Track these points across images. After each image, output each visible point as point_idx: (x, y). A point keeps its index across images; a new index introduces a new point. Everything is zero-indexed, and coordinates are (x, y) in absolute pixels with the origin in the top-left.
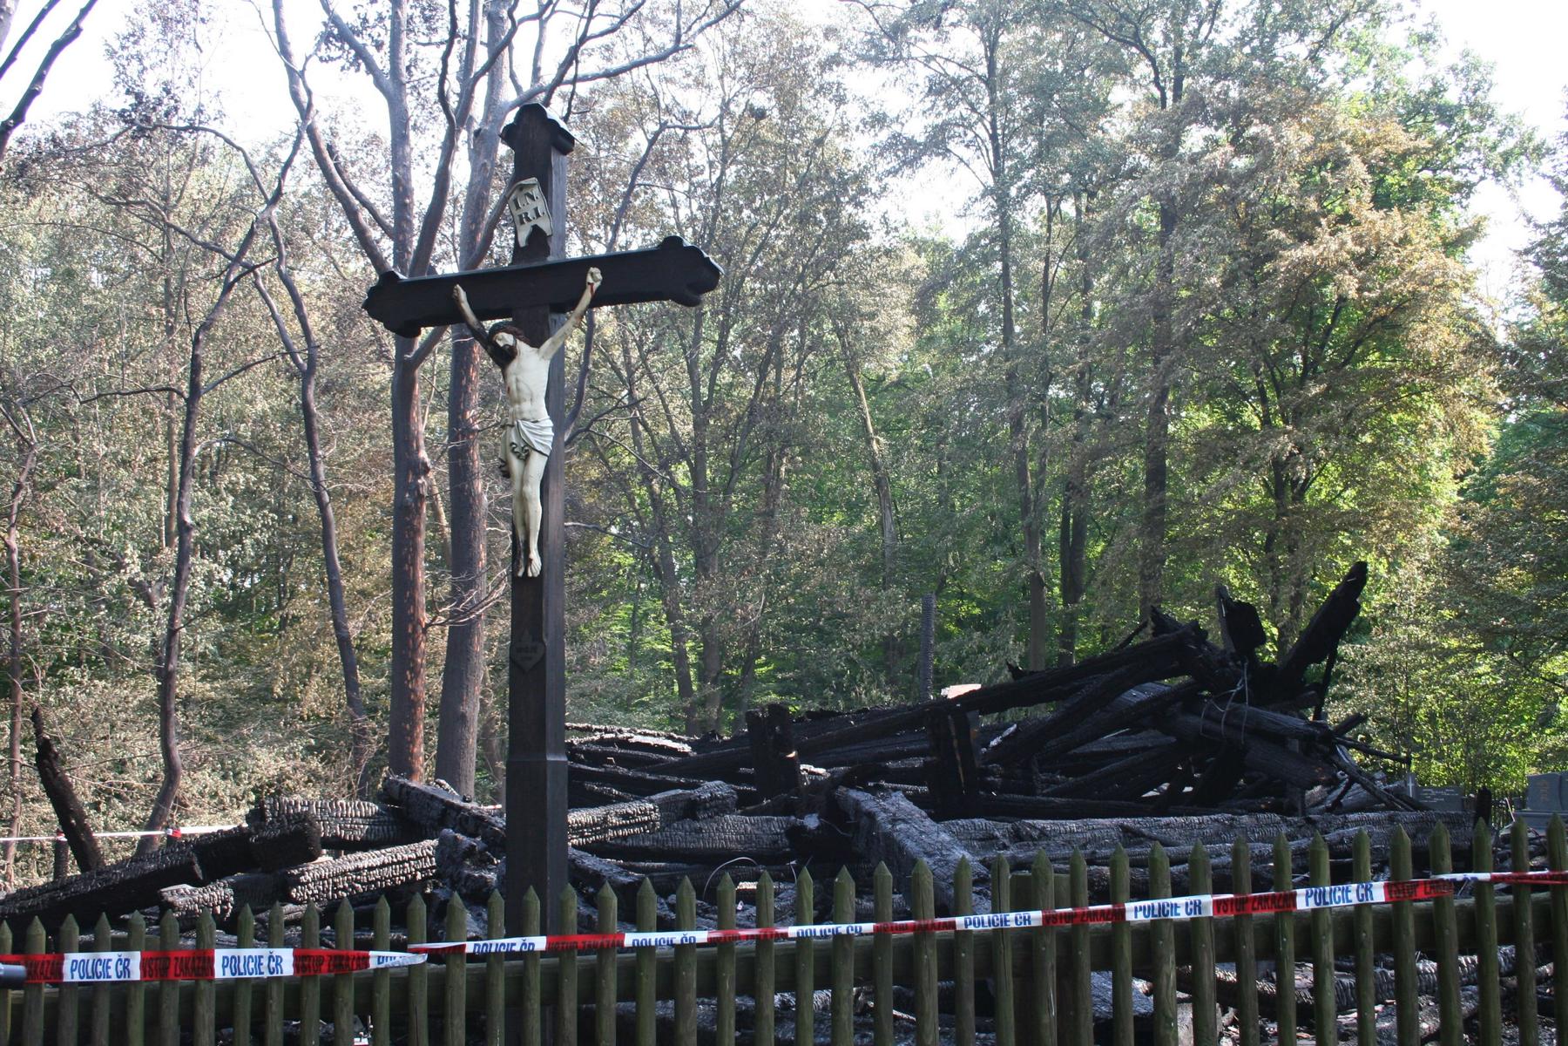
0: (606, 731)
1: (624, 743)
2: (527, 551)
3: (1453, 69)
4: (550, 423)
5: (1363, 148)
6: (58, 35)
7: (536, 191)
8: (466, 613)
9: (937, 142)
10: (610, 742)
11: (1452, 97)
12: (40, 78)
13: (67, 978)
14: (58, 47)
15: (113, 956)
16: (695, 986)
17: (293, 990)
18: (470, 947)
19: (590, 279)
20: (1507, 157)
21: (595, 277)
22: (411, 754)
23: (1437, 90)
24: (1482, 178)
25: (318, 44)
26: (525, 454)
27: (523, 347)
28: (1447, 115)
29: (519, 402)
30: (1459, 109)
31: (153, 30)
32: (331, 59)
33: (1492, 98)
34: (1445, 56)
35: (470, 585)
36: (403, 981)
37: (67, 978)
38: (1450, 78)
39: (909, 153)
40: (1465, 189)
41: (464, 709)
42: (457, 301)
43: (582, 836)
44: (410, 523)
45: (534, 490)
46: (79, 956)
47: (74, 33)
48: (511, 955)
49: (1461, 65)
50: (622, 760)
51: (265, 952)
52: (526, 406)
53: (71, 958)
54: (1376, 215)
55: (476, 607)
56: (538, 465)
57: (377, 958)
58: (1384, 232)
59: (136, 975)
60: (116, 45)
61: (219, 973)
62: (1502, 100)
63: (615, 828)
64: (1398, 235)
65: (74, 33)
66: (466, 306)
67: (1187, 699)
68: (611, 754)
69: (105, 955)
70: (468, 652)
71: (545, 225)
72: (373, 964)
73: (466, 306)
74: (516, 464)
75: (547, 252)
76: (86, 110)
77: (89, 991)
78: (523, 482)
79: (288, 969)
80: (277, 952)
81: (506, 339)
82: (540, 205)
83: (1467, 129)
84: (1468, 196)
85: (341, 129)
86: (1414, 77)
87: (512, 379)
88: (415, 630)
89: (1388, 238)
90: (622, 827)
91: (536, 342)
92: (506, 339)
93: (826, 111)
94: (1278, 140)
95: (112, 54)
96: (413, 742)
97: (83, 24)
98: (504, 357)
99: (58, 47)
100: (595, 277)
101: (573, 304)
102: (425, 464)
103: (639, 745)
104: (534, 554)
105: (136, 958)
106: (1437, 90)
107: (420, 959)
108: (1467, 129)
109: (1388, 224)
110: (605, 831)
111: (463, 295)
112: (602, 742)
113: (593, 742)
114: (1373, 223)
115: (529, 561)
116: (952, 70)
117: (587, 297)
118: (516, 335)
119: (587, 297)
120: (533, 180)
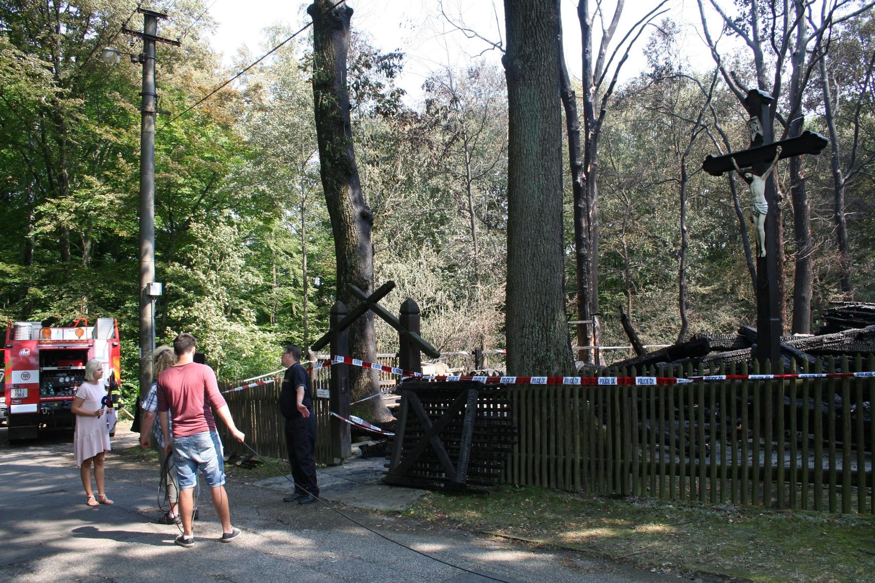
0: (851, 304)
1: (859, 309)
2: (761, 248)
4: (766, 203)
6: (620, 60)
7: (757, 121)
8: (802, 255)
10: (852, 308)
12: (616, 76)
14: (621, 64)
16: (771, 391)
17: (657, 389)
18: (704, 378)
19: (777, 150)
21: (779, 149)
22: (781, 314)
26: (758, 214)
27: (755, 177)
29: (754, 196)
31: (660, 40)
32: (731, 34)
35: (804, 244)
36: (686, 387)
41: (805, 295)
42: (732, 163)
43: (812, 346)
45: (761, 227)
46: (602, 378)
47: (626, 57)
48: (716, 380)
50: (856, 316)
51: (649, 378)
52: (757, 198)
53: (600, 378)
55: (808, 251)
56: (762, 218)
57: (679, 380)
59: (616, 383)
60: (647, 49)
61: (637, 384)
63: (826, 343)
65: (626, 57)
66: (735, 164)
68: (851, 313)
69: (608, 378)
70: (804, 271)
71: (761, 132)
72: (678, 382)
73: (735, 164)
74: (755, 218)
75: (762, 141)
76: (638, 75)
77: (605, 387)
78: (758, 224)
79: (655, 383)
80: (652, 378)
81: (749, 175)
82: (759, 126)
85: (741, 60)
88: (780, 264)
90: (829, 343)
91: (760, 174)
92: (749, 175)
95: (645, 53)
96: (781, 309)
97: (628, 54)
98: (750, 181)
99: (621, 64)
100: (779, 149)
102: (780, 196)
103: (866, 309)
104: (764, 249)
105: (616, 379)
107: (691, 381)
110: (822, 344)
111: (734, 161)
112: (849, 308)
113: (844, 309)
115: (761, 252)
117: (777, 157)
118: (753, 173)
119: (777, 157)
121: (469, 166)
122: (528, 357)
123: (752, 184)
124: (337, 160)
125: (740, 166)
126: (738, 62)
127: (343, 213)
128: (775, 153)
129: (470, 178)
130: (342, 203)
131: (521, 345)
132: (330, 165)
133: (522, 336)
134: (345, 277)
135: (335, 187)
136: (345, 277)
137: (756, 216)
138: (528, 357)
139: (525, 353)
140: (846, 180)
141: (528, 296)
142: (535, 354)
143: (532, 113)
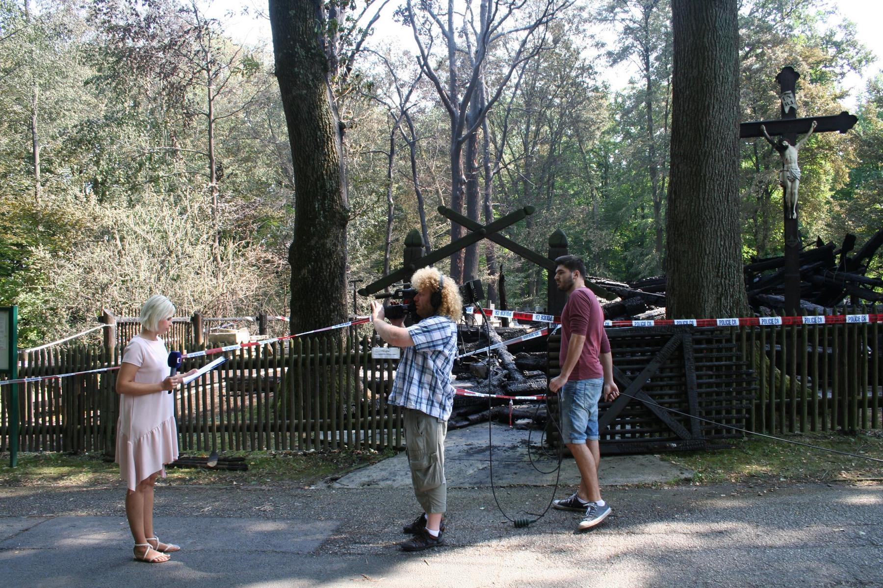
1: (603, 283)
3: (840, 26)
5: (806, 59)
6: (371, 19)
7: (791, 95)
9: (624, 53)
11: (837, 38)
13: (847, 322)
15: (860, 316)
20: (860, 62)
21: (814, 124)
23: (832, 34)
24: (849, 71)
25: (394, 16)
26: (793, 181)
28: (837, 45)
30: (842, 43)
33: (857, 37)
34: (833, 22)
37: (847, 322)
38: (838, 29)
39: (616, 58)
40: (843, 75)
42: (763, 130)
44: (459, 203)
46: (850, 316)
47: (377, 17)
49: (844, 24)
52: (793, 165)
54: (811, 86)
58: (815, 93)
59: (867, 321)
62: (860, 38)
64: (820, 94)
67: (817, 271)
69: (858, 316)
74: (789, 184)
77: (853, 325)
81: (786, 143)
83: (844, 50)
84: (842, 78)
85: (392, 48)
86: (821, 30)
87: (788, 157)
89: (816, 95)
91: (794, 144)
93: (576, 41)
94: (774, 55)
97: (380, 13)
100: (814, 124)
101: (807, 131)
105: (867, 316)
106: (832, 34)
108: (844, 50)
109: (815, 88)
114: (810, 89)
116: (631, 25)
117: (812, 130)
119: (812, 130)
120: (790, 92)
121: (212, 103)
122: (726, 299)
123: (787, 152)
124: (314, 49)
125: (770, 135)
126: (390, 50)
127: (321, 119)
128: (810, 126)
129: (212, 118)
130: (321, 107)
131: (717, 286)
132: (304, 53)
133: (718, 276)
134: (323, 204)
135: (310, 83)
136: (323, 204)
137: (790, 181)
138: (726, 299)
139: (722, 294)
140: (494, 174)
141: (723, 233)
142: (732, 296)
143: (728, 39)
